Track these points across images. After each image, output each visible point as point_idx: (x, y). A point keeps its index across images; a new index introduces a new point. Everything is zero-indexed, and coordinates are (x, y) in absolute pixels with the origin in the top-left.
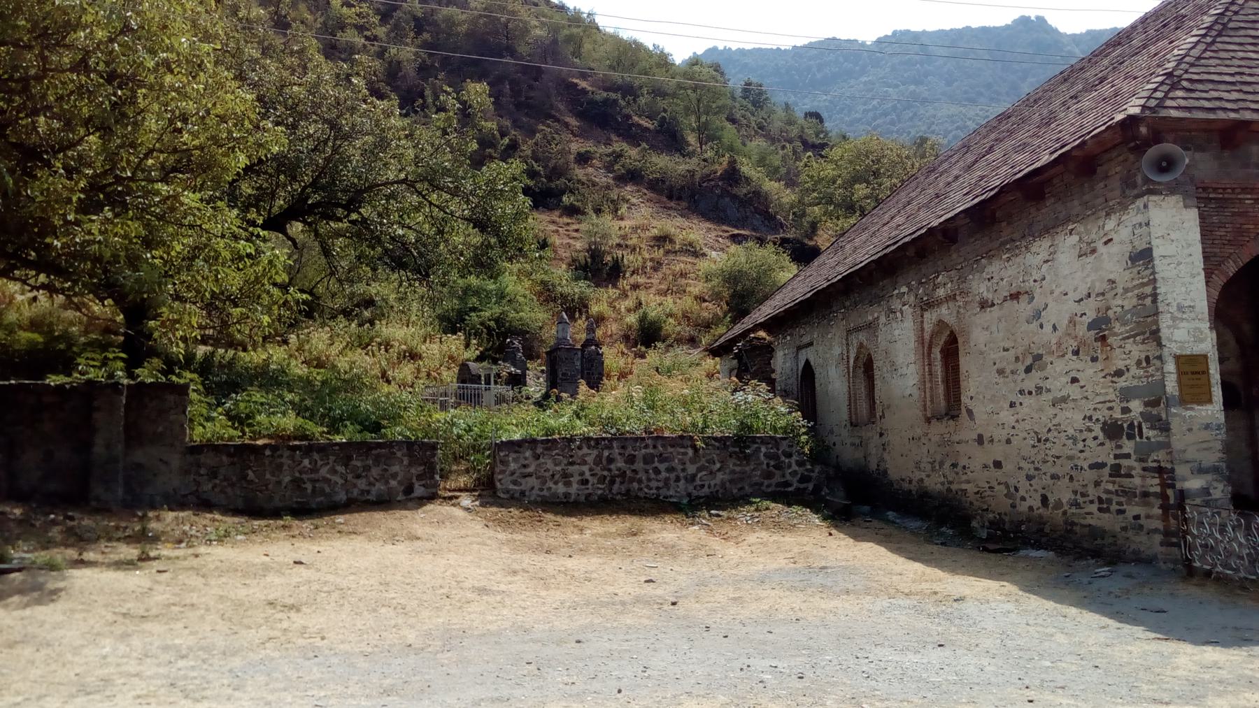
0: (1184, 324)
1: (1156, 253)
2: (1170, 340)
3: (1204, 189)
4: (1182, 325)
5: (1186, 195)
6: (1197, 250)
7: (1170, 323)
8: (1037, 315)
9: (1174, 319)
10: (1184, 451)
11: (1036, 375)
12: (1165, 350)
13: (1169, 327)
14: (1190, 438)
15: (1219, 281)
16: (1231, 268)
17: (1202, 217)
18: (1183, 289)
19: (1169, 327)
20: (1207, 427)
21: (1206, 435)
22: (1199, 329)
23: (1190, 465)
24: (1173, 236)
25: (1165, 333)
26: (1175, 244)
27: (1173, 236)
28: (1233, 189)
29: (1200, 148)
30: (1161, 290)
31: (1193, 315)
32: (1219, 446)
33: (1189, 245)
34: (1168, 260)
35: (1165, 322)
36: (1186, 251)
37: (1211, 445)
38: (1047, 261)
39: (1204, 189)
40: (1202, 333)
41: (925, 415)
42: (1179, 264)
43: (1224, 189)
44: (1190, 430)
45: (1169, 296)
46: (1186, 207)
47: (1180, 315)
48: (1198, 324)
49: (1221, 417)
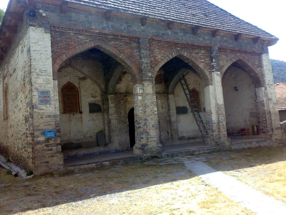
0: (42, 77)
1: (31, 49)
2: (35, 83)
3: (54, 27)
4: (41, 77)
5: (46, 28)
6: (49, 49)
7: (36, 76)
8: (17, 78)
9: (38, 75)
10: (39, 126)
11: (17, 100)
12: (33, 86)
13: (35, 78)
14: (42, 121)
15: (59, 62)
16: (64, 58)
17: (52, 37)
18: (42, 64)
19: (35, 78)
20: (49, 116)
21: (49, 119)
22: (48, 79)
23: (41, 131)
24: (39, 43)
25: (33, 80)
26: (40, 46)
27: (39, 43)
28: (66, 28)
29: (52, 11)
30: (33, 63)
31: (46, 74)
32: (53, 123)
33: (46, 47)
34: (37, 52)
35: (34, 76)
36: (45, 49)
37: (50, 123)
38: (17, 57)
39: (54, 27)
40: (49, 80)
41: (4, 118)
42: (41, 54)
43: (62, 28)
44: (42, 118)
45: (36, 66)
46: (45, 33)
47: (40, 74)
48: (48, 77)
49: (58, 113)
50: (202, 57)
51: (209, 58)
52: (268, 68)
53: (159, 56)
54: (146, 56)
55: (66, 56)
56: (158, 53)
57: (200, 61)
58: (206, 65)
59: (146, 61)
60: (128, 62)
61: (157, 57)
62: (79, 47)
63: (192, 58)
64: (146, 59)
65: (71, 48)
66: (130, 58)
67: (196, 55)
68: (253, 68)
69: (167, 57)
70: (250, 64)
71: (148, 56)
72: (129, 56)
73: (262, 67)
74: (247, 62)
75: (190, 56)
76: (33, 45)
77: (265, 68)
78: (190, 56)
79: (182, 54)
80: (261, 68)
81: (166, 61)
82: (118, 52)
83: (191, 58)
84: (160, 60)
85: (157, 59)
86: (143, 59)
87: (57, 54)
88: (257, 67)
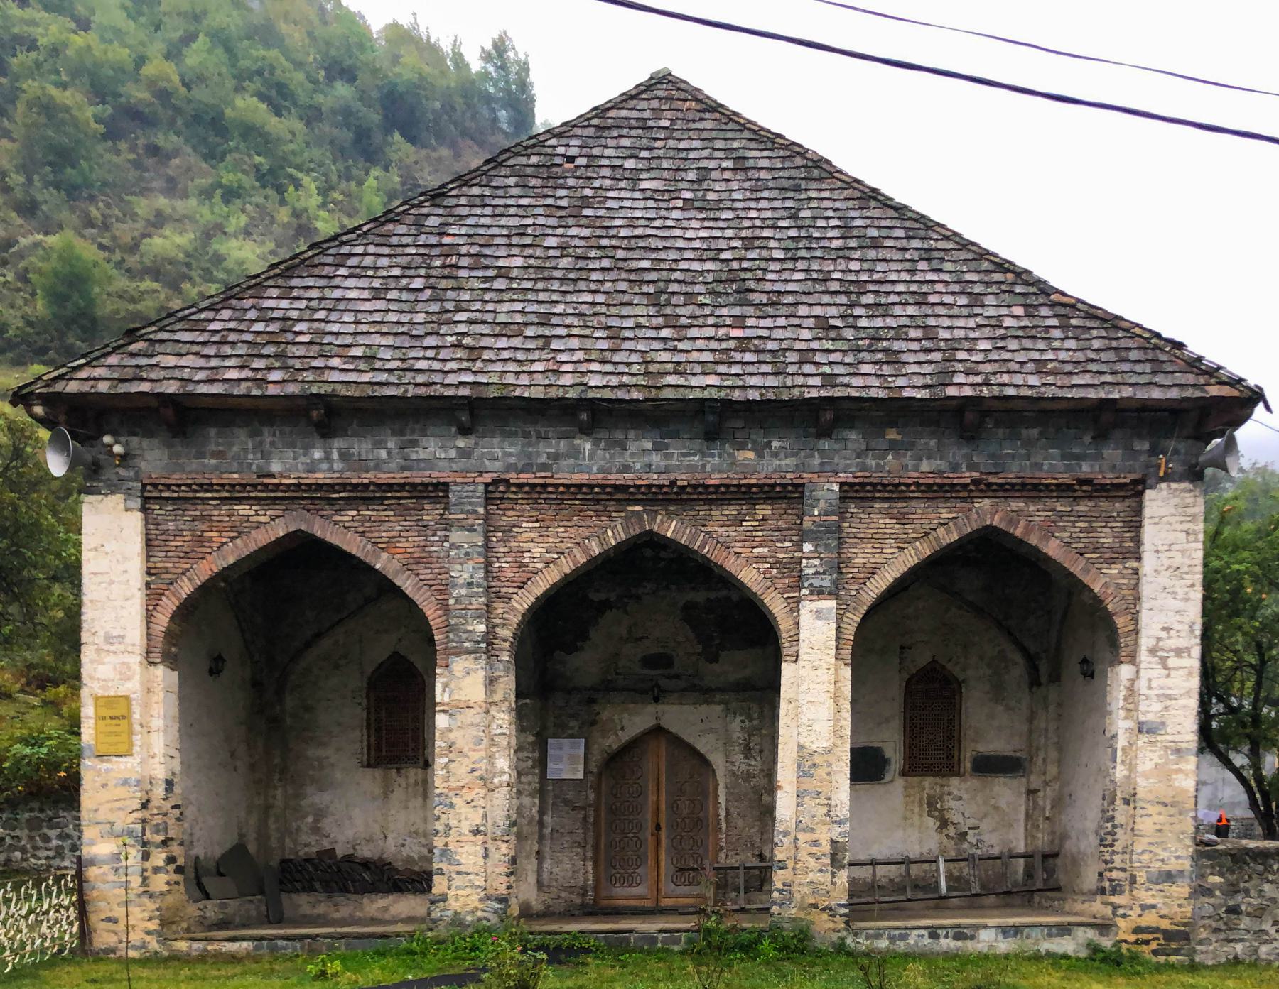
16: (186, 588)
34: (100, 578)
42: (112, 582)
50: (760, 534)
51: (794, 538)
52: (1178, 559)
53: (537, 550)
54: (467, 554)
55: (190, 580)
56: (533, 535)
57: (745, 555)
58: (775, 571)
59: (466, 575)
60: (406, 584)
61: (526, 554)
62: (235, 545)
63: (703, 545)
64: (469, 566)
65: (209, 550)
66: (414, 567)
67: (723, 529)
68: (1076, 568)
69: (576, 551)
70: (1052, 549)
71: (479, 554)
72: (411, 561)
73: (1139, 559)
74: (1033, 540)
75: (694, 537)
76: (93, 554)
77: (1149, 563)
78: (694, 537)
79: (655, 528)
80: (1135, 565)
81: (567, 566)
82: (369, 546)
83: (698, 544)
84: (540, 566)
85: (527, 560)
86: (459, 567)
87: (164, 576)
88: (1110, 562)
